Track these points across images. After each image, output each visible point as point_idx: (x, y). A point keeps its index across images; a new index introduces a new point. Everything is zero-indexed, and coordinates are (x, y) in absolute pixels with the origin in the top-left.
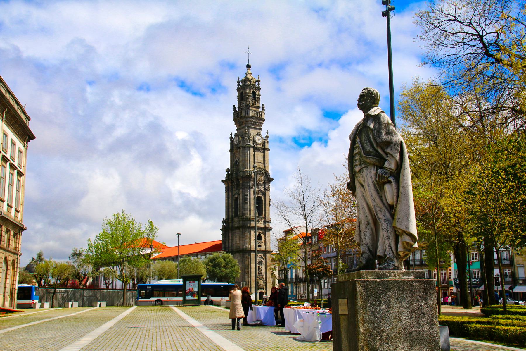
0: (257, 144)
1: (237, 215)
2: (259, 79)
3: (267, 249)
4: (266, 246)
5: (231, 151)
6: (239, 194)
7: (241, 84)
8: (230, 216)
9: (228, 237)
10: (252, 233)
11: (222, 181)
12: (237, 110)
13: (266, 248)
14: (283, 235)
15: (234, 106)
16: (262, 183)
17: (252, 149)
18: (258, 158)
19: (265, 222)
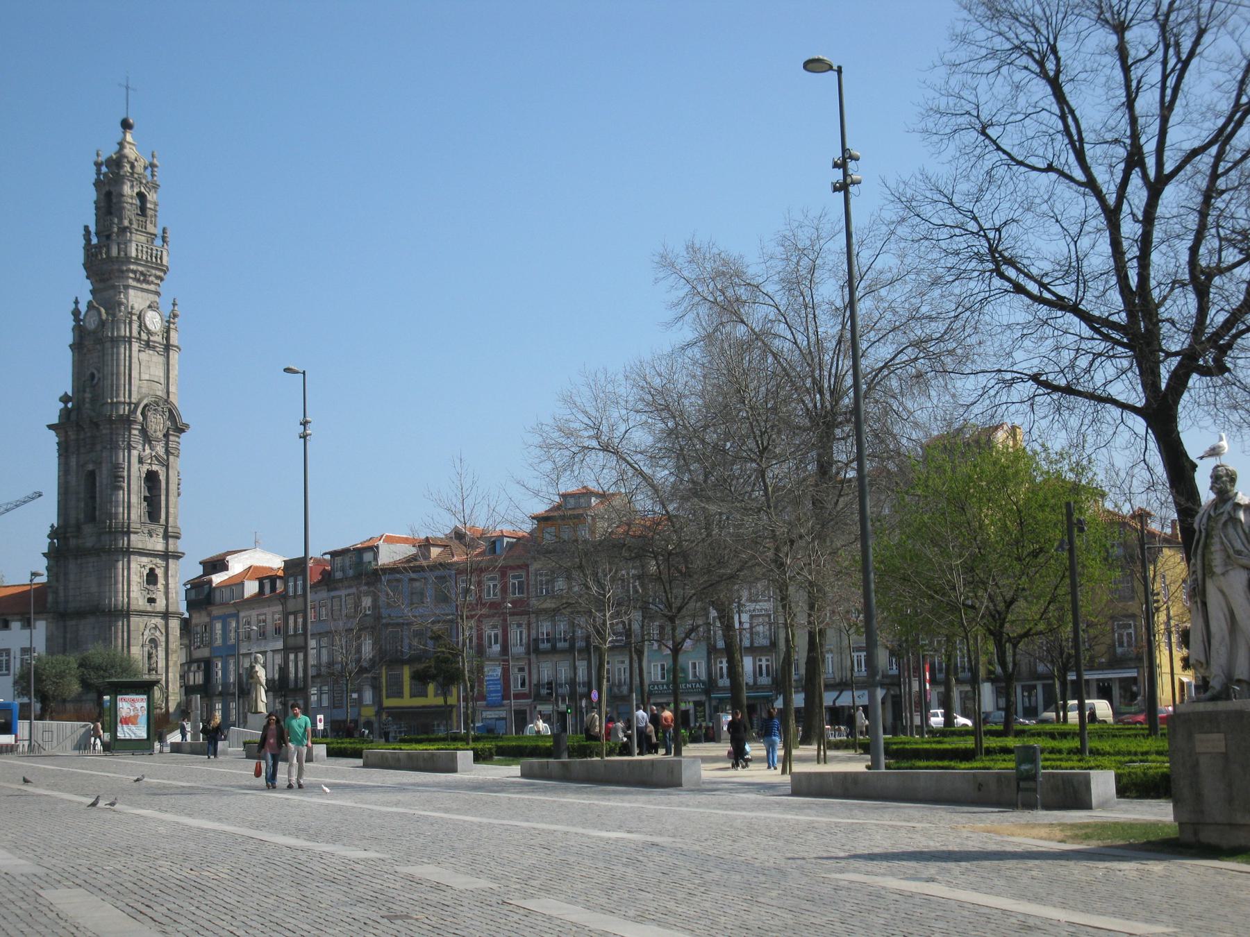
0: (149, 333)
2: (155, 161)
4: (167, 599)
7: (104, 169)
8: (72, 521)
9: (66, 574)
10: (133, 565)
11: (50, 427)
12: (94, 241)
13: (167, 606)
14: (199, 571)
15: (86, 228)
16: (160, 435)
17: (135, 346)
18: (153, 371)
19: (166, 536)
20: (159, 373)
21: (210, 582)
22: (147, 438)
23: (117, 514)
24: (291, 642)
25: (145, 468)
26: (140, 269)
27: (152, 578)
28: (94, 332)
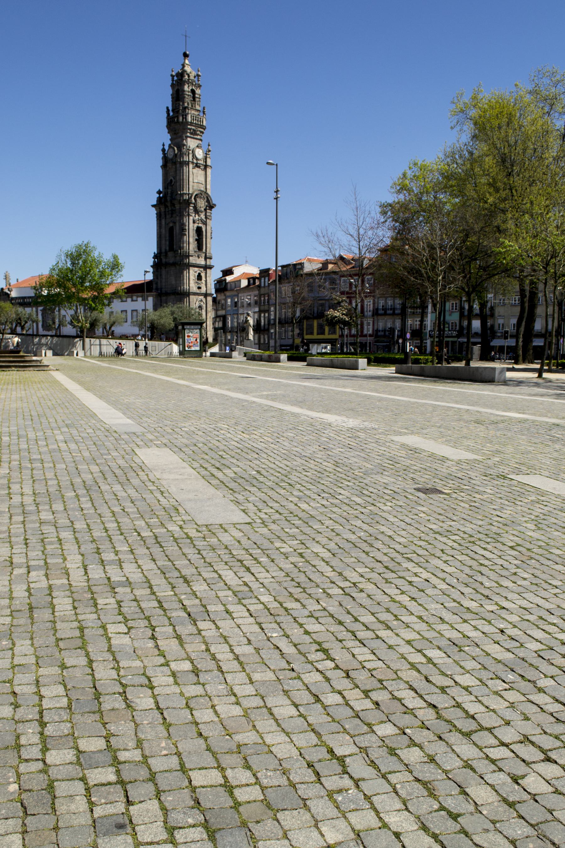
1: (171, 248)
2: (199, 73)
3: (208, 292)
5: (164, 166)
6: (175, 223)
7: (175, 78)
8: (163, 250)
9: (161, 275)
10: (191, 271)
11: (153, 206)
12: (171, 114)
14: (220, 275)
15: (167, 108)
16: (203, 209)
17: (191, 166)
18: (199, 178)
20: (202, 179)
21: (225, 280)
22: (197, 211)
23: (183, 247)
24: (262, 308)
25: (196, 225)
26: (193, 128)
27: (199, 277)
28: (172, 159)
